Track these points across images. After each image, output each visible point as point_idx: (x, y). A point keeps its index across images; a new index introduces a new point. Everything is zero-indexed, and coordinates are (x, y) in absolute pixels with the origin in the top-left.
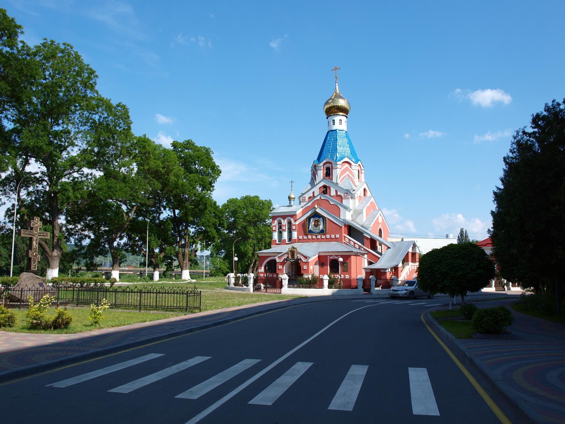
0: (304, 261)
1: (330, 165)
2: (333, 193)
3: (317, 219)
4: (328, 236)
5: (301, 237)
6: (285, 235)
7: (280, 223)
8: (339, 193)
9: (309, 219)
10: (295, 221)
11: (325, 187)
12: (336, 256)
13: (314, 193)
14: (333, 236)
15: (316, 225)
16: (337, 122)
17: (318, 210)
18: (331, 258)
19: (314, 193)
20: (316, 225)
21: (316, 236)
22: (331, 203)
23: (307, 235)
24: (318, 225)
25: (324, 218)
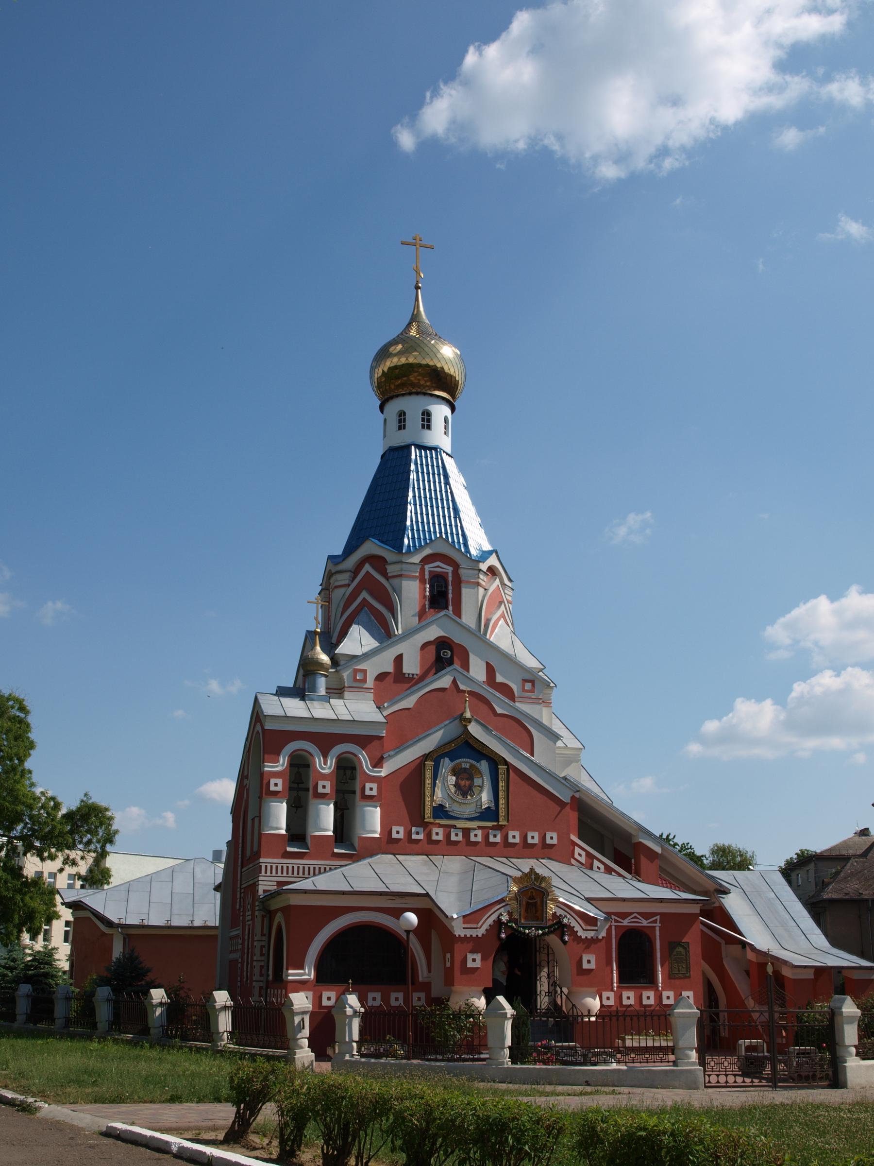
0: (581, 933)
1: (450, 569)
2: (477, 671)
3: (465, 763)
4: (514, 836)
5: (398, 832)
6: (325, 818)
7: (300, 767)
8: (499, 679)
9: (435, 756)
10: (378, 763)
11: (442, 644)
12: (646, 916)
13: (399, 660)
14: (534, 838)
15: (465, 790)
16: (438, 422)
17: (474, 729)
18: (626, 922)
19: (399, 660)
20: (465, 790)
21: (466, 832)
22: (499, 710)
23: (425, 825)
24: (470, 788)
25: (495, 761)
